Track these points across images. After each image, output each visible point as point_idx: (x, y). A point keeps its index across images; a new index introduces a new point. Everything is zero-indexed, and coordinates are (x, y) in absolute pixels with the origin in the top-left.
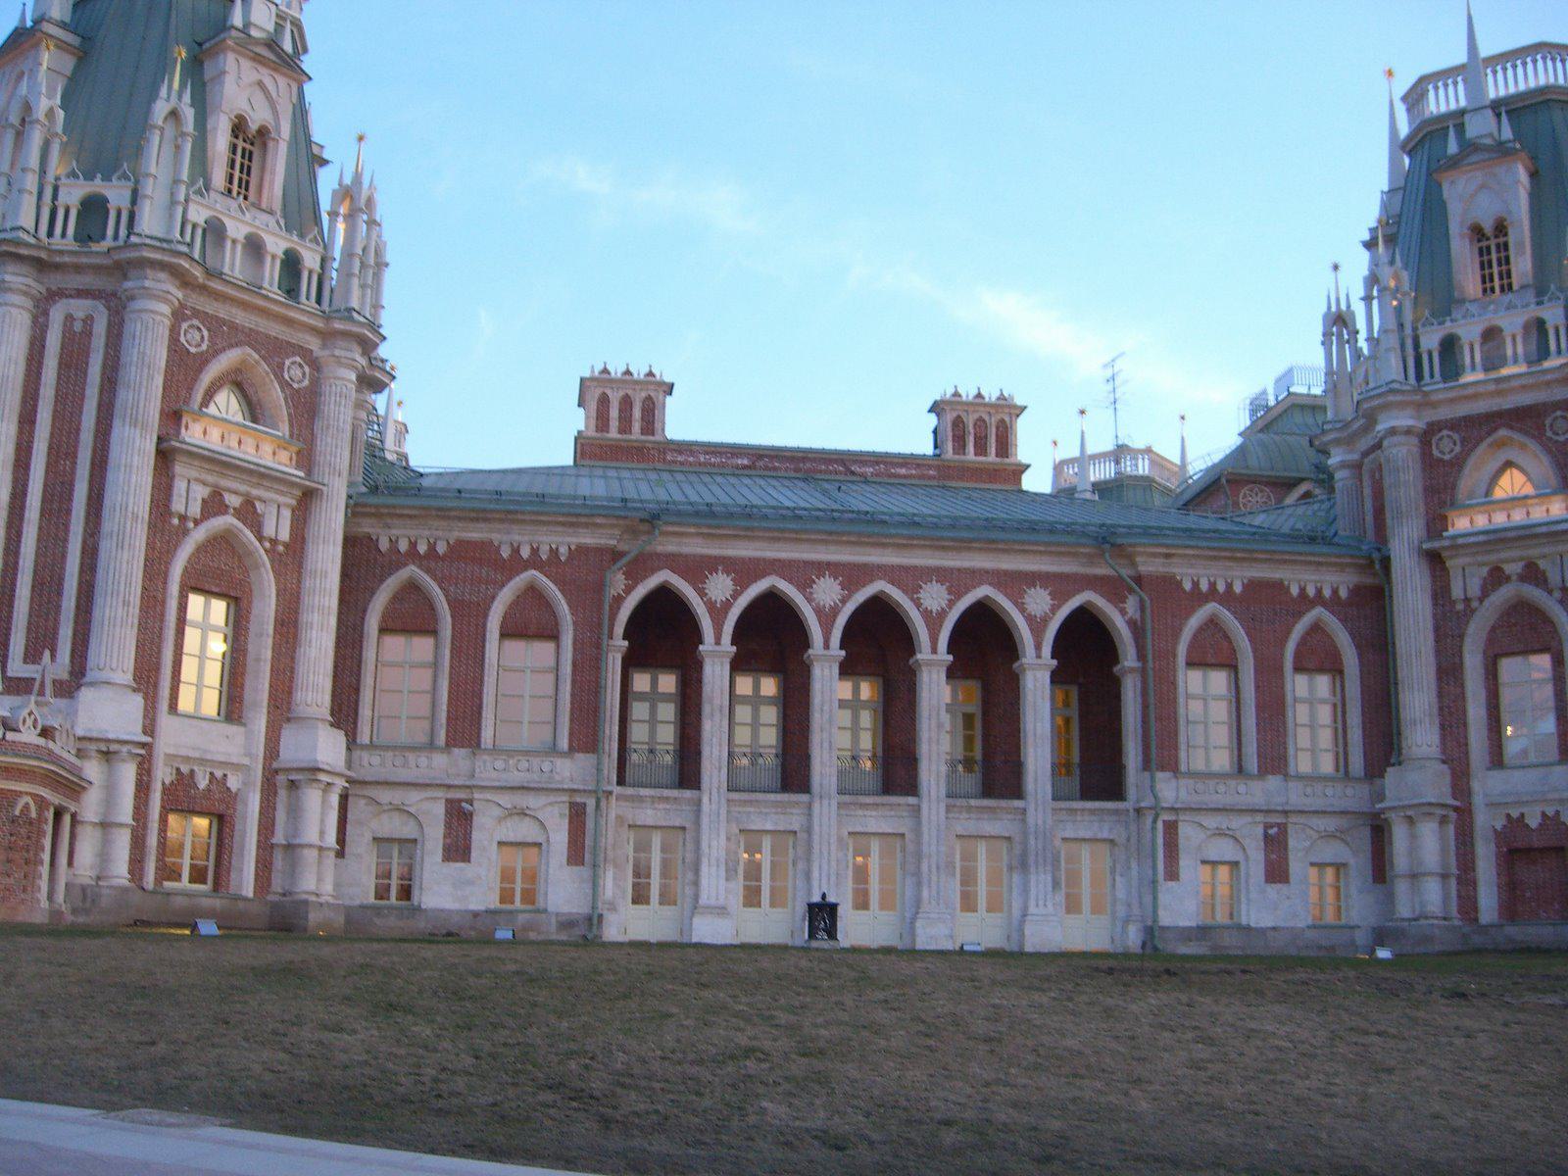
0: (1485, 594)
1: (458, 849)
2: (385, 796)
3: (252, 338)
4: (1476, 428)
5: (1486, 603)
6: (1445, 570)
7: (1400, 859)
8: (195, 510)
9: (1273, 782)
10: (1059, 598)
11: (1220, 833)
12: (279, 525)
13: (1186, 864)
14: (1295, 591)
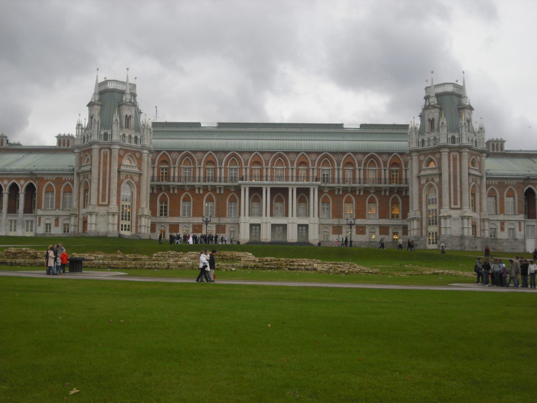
9: (57, 210)
10: (26, 181)
11: (48, 219)
14: (64, 179)
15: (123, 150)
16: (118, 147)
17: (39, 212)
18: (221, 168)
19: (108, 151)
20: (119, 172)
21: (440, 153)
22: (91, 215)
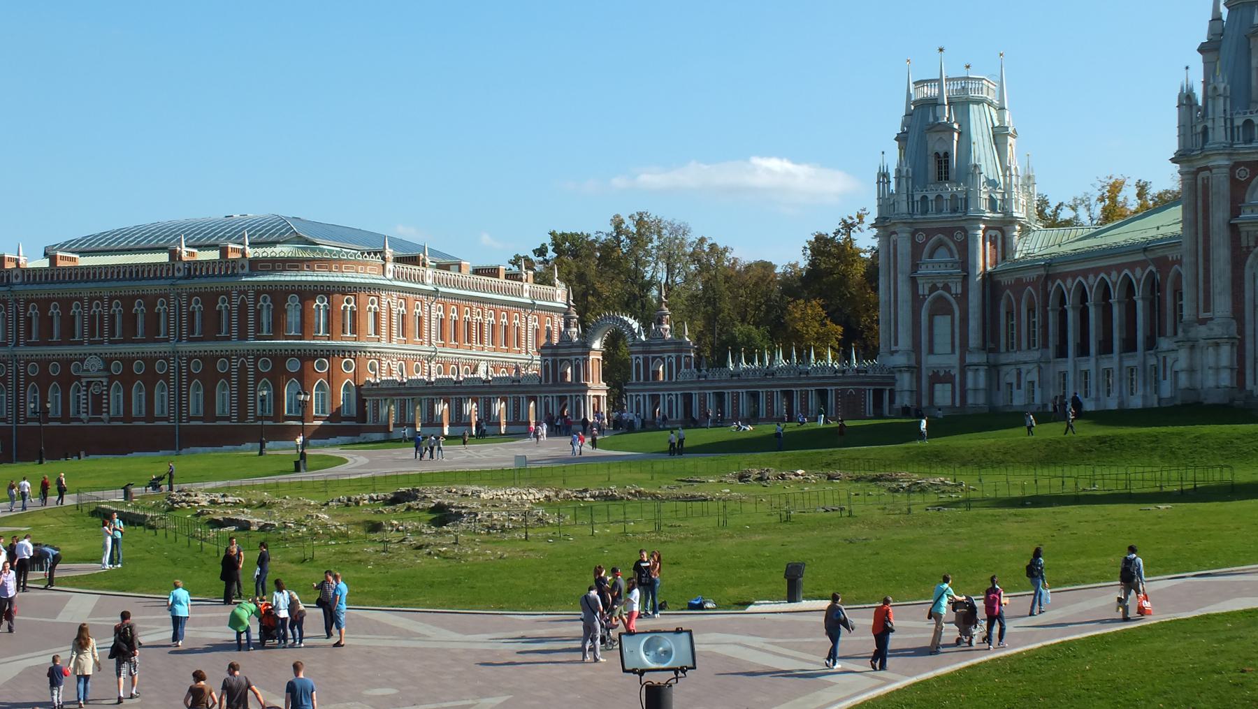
1: (1019, 387)
2: (1005, 369)
3: (940, 230)
8: (927, 292)
12: (957, 288)
13: (1168, 373)
15: (1247, 164)
16: (1223, 161)
17: (1164, 343)
19: (1207, 173)
20: (1234, 229)
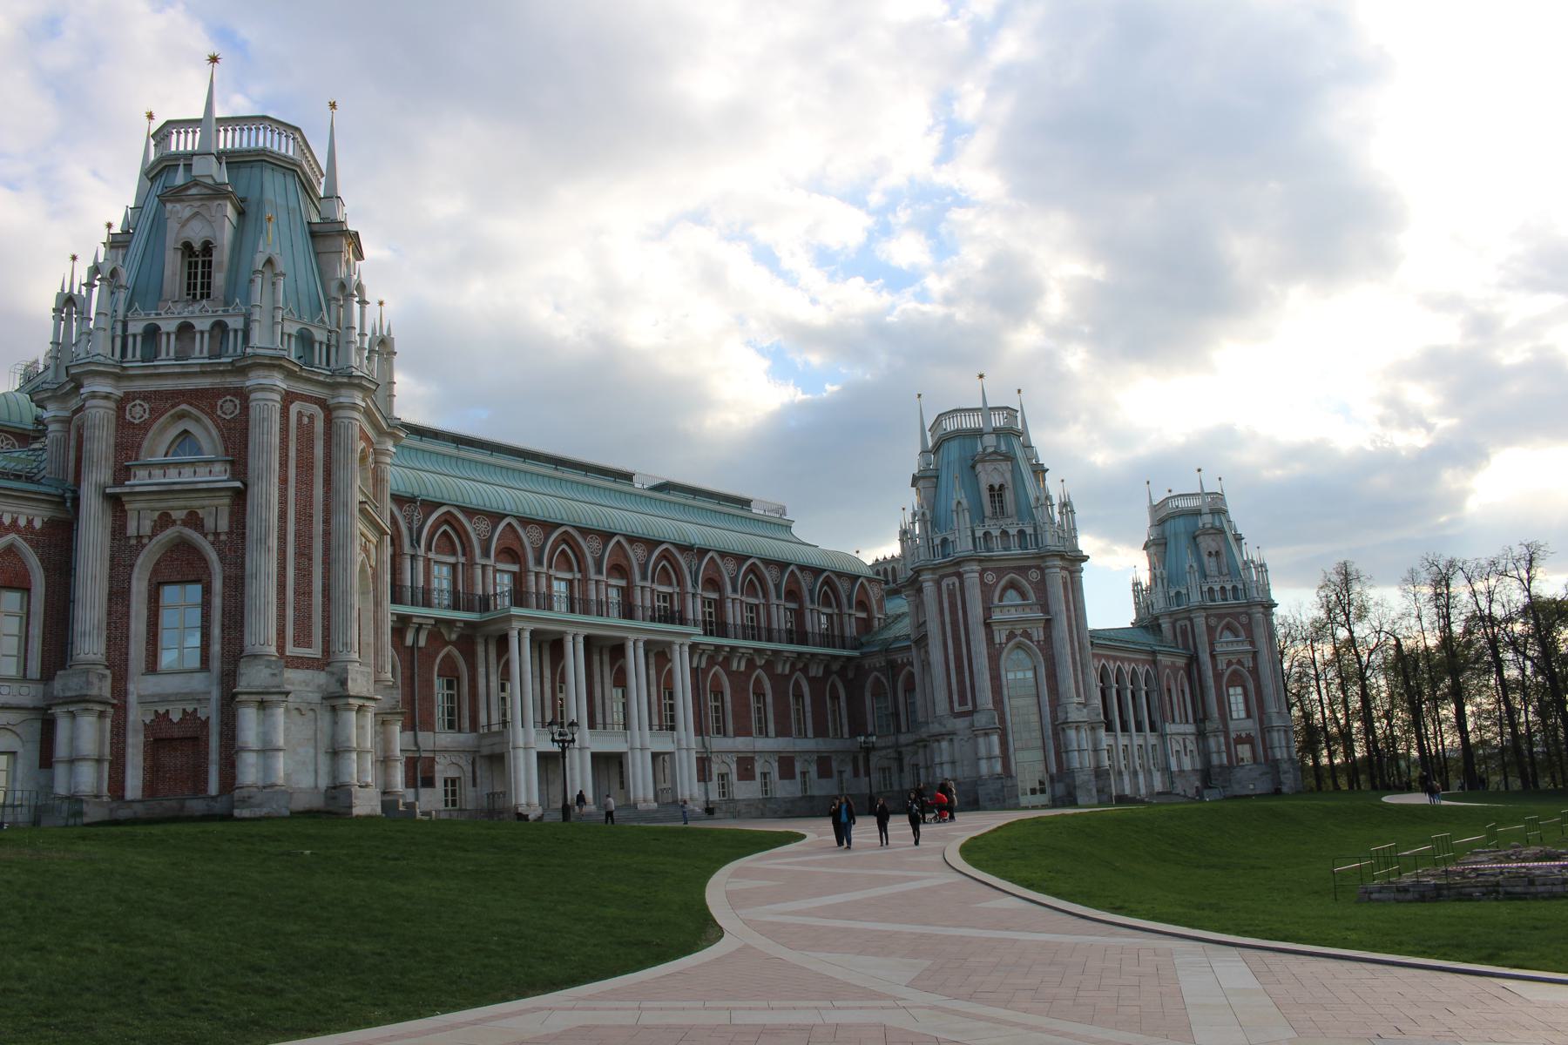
0: (154, 534)
4: (161, 401)
5: (154, 540)
6: (124, 511)
7: (61, 750)
18: (413, 557)
21: (1042, 569)
22: (263, 705)
